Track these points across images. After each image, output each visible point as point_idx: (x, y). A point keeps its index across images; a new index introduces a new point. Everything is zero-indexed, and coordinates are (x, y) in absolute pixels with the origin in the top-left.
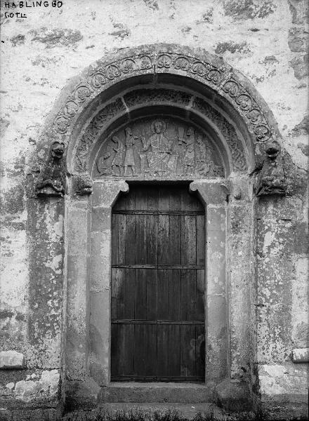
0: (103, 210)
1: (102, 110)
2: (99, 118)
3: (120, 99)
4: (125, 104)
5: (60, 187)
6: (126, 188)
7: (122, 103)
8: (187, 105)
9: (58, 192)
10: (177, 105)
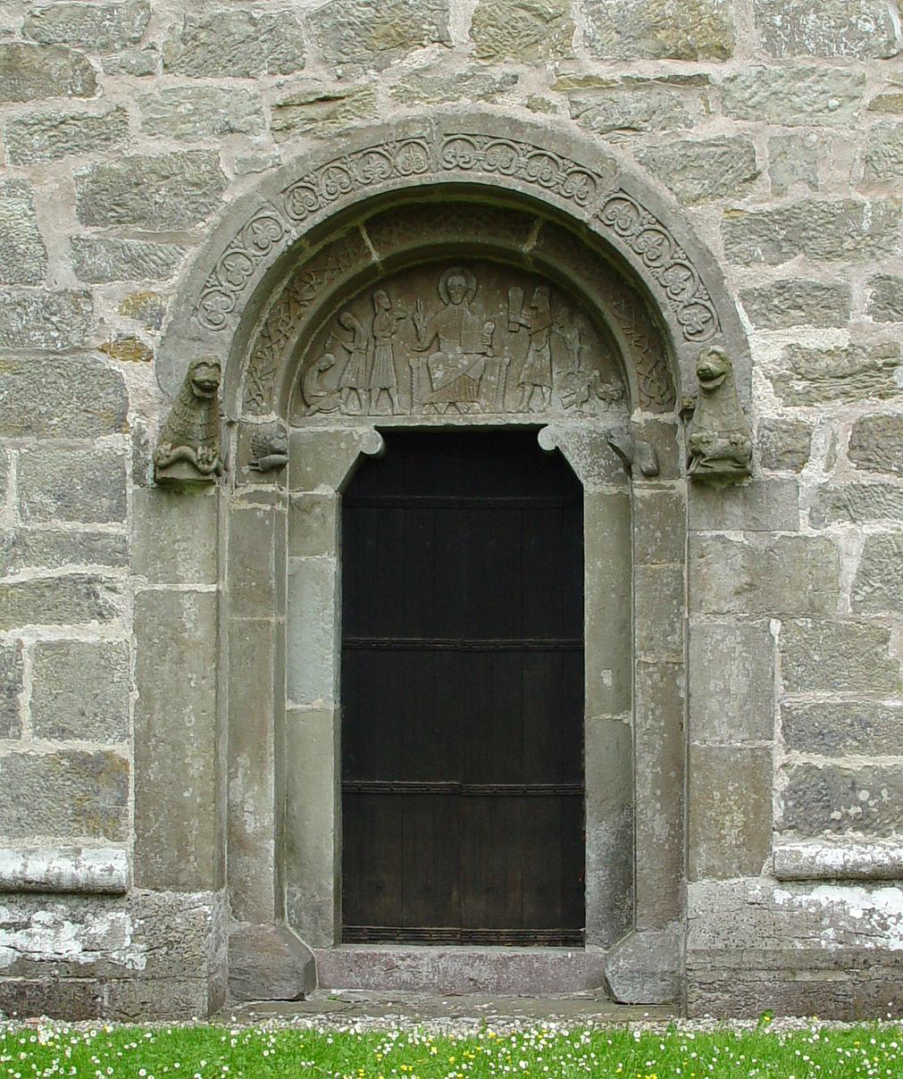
0: (316, 502)
1: (314, 259)
2: (302, 276)
3: (356, 231)
4: (368, 242)
5: (209, 463)
6: (375, 446)
7: (363, 240)
8: (524, 241)
9: (207, 474)
10: (499, 242)
